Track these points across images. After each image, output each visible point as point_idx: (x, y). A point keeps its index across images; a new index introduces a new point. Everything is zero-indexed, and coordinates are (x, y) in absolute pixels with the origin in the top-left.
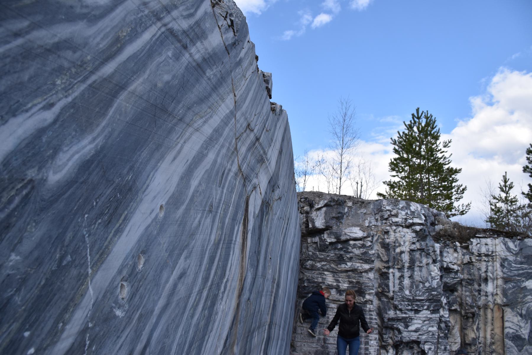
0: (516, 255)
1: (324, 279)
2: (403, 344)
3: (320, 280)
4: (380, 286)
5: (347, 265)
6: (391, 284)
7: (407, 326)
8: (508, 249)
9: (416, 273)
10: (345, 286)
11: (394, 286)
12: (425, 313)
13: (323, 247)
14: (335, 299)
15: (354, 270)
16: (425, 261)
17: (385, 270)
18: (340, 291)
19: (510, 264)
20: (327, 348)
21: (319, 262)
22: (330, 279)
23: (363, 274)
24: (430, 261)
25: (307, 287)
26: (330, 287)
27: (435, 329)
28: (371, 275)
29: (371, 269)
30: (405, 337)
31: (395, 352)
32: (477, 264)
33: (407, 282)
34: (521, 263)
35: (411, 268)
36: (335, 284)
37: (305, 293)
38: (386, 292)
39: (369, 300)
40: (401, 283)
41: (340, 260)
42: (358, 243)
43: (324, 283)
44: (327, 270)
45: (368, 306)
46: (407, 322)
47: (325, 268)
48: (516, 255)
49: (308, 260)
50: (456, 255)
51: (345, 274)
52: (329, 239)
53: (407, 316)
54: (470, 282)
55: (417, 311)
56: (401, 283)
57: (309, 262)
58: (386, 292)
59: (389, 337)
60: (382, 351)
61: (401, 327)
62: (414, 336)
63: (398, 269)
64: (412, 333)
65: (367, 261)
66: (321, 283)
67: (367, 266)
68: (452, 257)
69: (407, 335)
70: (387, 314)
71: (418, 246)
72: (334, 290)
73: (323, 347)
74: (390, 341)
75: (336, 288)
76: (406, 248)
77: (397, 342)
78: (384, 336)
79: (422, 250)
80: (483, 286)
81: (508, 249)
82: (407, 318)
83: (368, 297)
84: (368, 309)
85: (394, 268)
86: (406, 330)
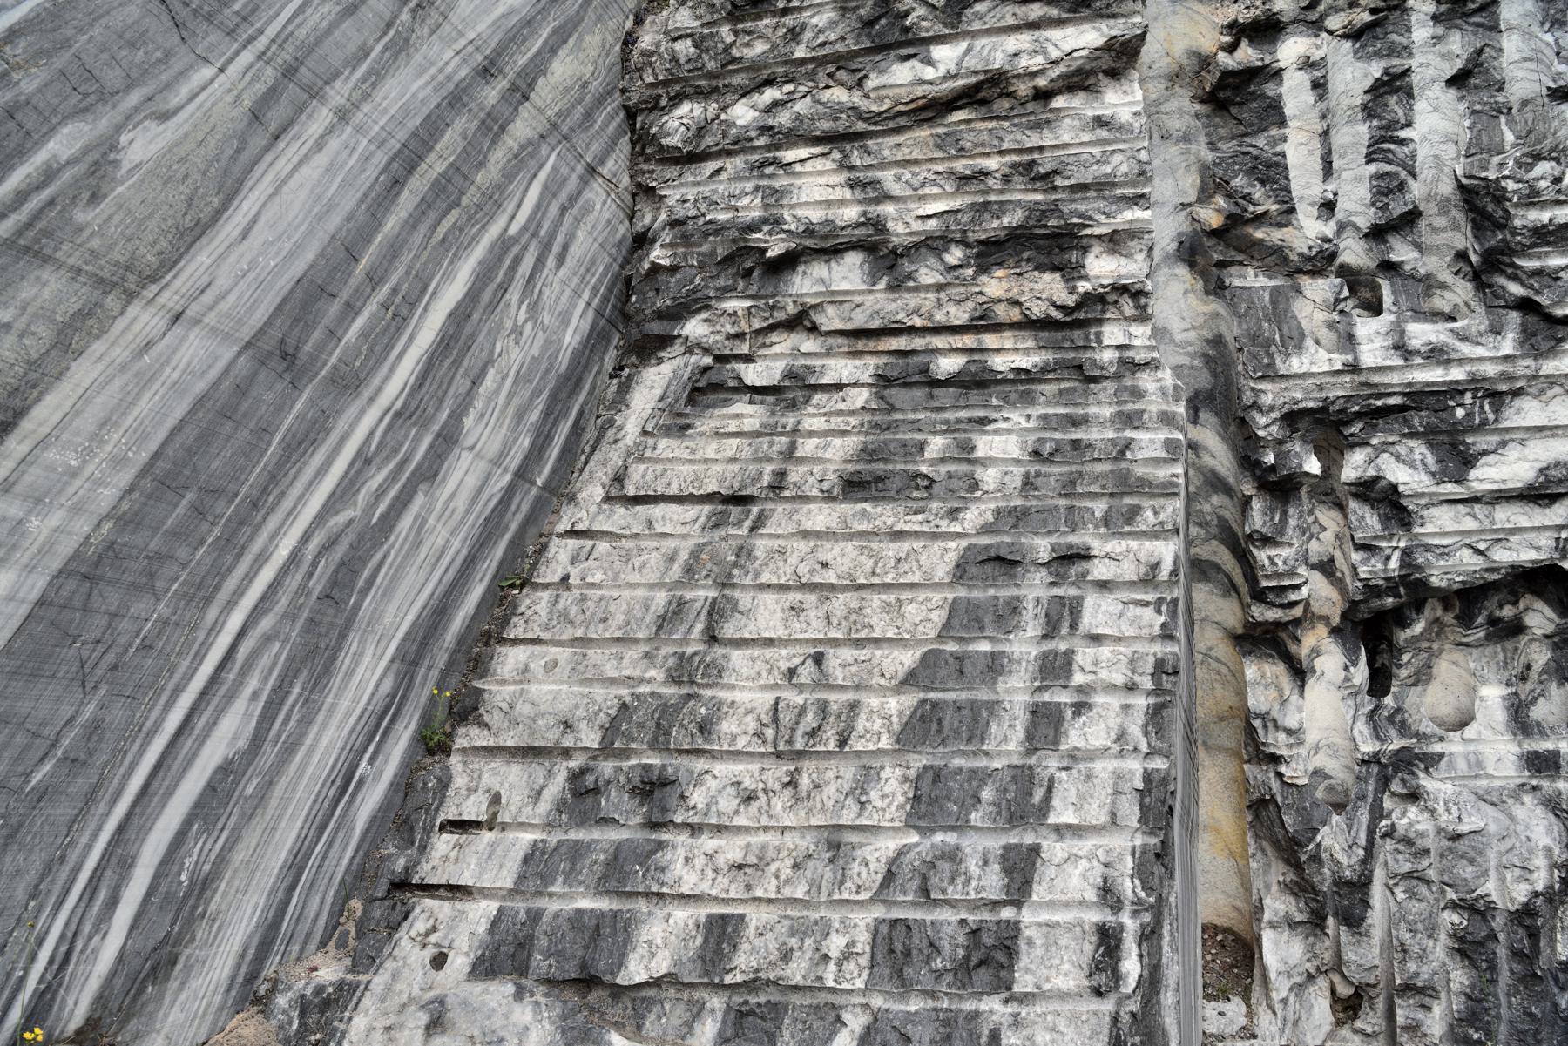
1: (775, 196)
2: (1433, 609)
3: (752, 209)
4: (1212, 184)
5: (929, 62)
6: (1298, 150)
7: (1457, 458)
9: (1511, 45)
11: (1328, 170)
14: (859, 320)
15: (985, 92)
17: (1248, 54)
18: (887, 258)
20: (716, 672)
21: (745, 93)
22: (817, 190)
23: (1059, 102)
25: (673, 269)
26: (824, 245)
28: (1121, 101)
30: (1444, 552)
31: (1361, 674)
36: (851, 213)
37: (660, 315)
38: (1260, 219)
39: (1123, 289)
40: (1386, 142)
43: (777, 221)
44: (794, 137)
45: (1113, 334)
47: (784, 118)
49: (677, 100)
51: (924, 133)
53: (1457, 374)
56: (1386, 142)
57: (684, 108)
58: (1260, 219)
59: (1304, 558)
60: (1251, 671)
61: (1406, 467)
63: (1354, 34)
64: (1507, 515)
66: (753, 227)
70: (1270, 375)
72: (854, 259)
73: (682, 671)
74: (1318, 591)
75: (868, 247)
77: (1372, 591)
78: (1262, 555)
82: (1454, 391)
83: (1101, 268)
84: (1108, 356)
85: (1317, 27)
86: (1450, 488)
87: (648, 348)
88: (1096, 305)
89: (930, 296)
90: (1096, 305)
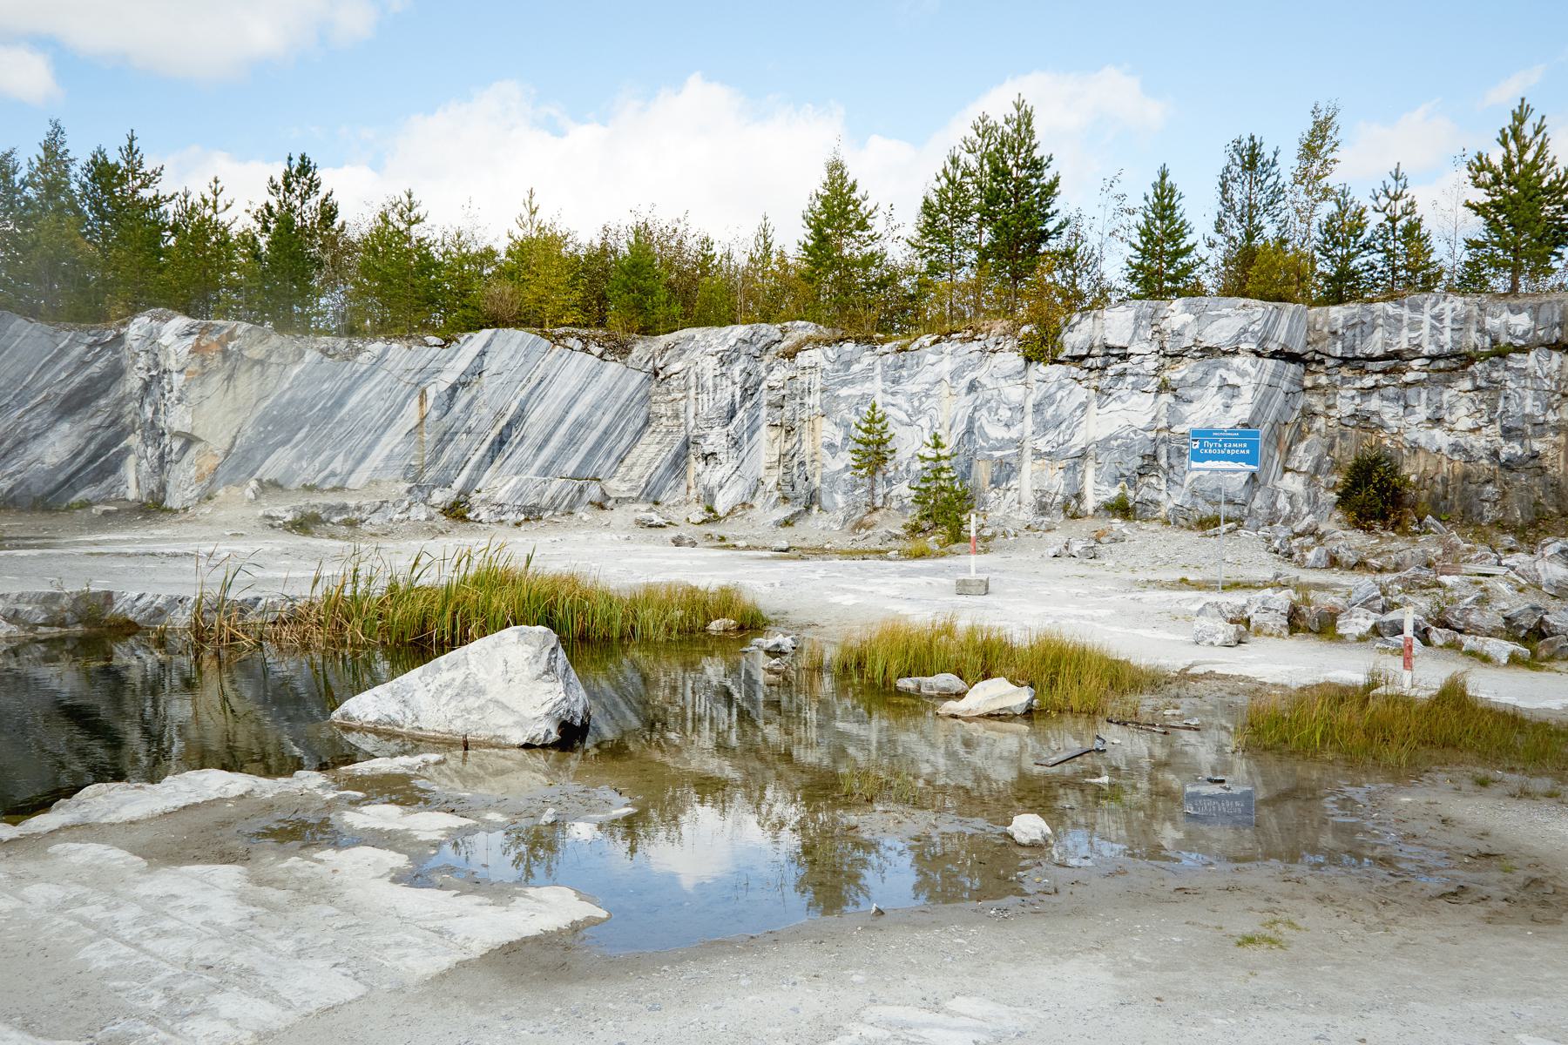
12: (717, 429)
32: (801, 378)
41: (668, 393)
52: (661, 376)
54: (793, 396)
68: (779, 375)
69: (708, 450)
76: (709, 374)
79: (723, 374)
80: (806, 400)
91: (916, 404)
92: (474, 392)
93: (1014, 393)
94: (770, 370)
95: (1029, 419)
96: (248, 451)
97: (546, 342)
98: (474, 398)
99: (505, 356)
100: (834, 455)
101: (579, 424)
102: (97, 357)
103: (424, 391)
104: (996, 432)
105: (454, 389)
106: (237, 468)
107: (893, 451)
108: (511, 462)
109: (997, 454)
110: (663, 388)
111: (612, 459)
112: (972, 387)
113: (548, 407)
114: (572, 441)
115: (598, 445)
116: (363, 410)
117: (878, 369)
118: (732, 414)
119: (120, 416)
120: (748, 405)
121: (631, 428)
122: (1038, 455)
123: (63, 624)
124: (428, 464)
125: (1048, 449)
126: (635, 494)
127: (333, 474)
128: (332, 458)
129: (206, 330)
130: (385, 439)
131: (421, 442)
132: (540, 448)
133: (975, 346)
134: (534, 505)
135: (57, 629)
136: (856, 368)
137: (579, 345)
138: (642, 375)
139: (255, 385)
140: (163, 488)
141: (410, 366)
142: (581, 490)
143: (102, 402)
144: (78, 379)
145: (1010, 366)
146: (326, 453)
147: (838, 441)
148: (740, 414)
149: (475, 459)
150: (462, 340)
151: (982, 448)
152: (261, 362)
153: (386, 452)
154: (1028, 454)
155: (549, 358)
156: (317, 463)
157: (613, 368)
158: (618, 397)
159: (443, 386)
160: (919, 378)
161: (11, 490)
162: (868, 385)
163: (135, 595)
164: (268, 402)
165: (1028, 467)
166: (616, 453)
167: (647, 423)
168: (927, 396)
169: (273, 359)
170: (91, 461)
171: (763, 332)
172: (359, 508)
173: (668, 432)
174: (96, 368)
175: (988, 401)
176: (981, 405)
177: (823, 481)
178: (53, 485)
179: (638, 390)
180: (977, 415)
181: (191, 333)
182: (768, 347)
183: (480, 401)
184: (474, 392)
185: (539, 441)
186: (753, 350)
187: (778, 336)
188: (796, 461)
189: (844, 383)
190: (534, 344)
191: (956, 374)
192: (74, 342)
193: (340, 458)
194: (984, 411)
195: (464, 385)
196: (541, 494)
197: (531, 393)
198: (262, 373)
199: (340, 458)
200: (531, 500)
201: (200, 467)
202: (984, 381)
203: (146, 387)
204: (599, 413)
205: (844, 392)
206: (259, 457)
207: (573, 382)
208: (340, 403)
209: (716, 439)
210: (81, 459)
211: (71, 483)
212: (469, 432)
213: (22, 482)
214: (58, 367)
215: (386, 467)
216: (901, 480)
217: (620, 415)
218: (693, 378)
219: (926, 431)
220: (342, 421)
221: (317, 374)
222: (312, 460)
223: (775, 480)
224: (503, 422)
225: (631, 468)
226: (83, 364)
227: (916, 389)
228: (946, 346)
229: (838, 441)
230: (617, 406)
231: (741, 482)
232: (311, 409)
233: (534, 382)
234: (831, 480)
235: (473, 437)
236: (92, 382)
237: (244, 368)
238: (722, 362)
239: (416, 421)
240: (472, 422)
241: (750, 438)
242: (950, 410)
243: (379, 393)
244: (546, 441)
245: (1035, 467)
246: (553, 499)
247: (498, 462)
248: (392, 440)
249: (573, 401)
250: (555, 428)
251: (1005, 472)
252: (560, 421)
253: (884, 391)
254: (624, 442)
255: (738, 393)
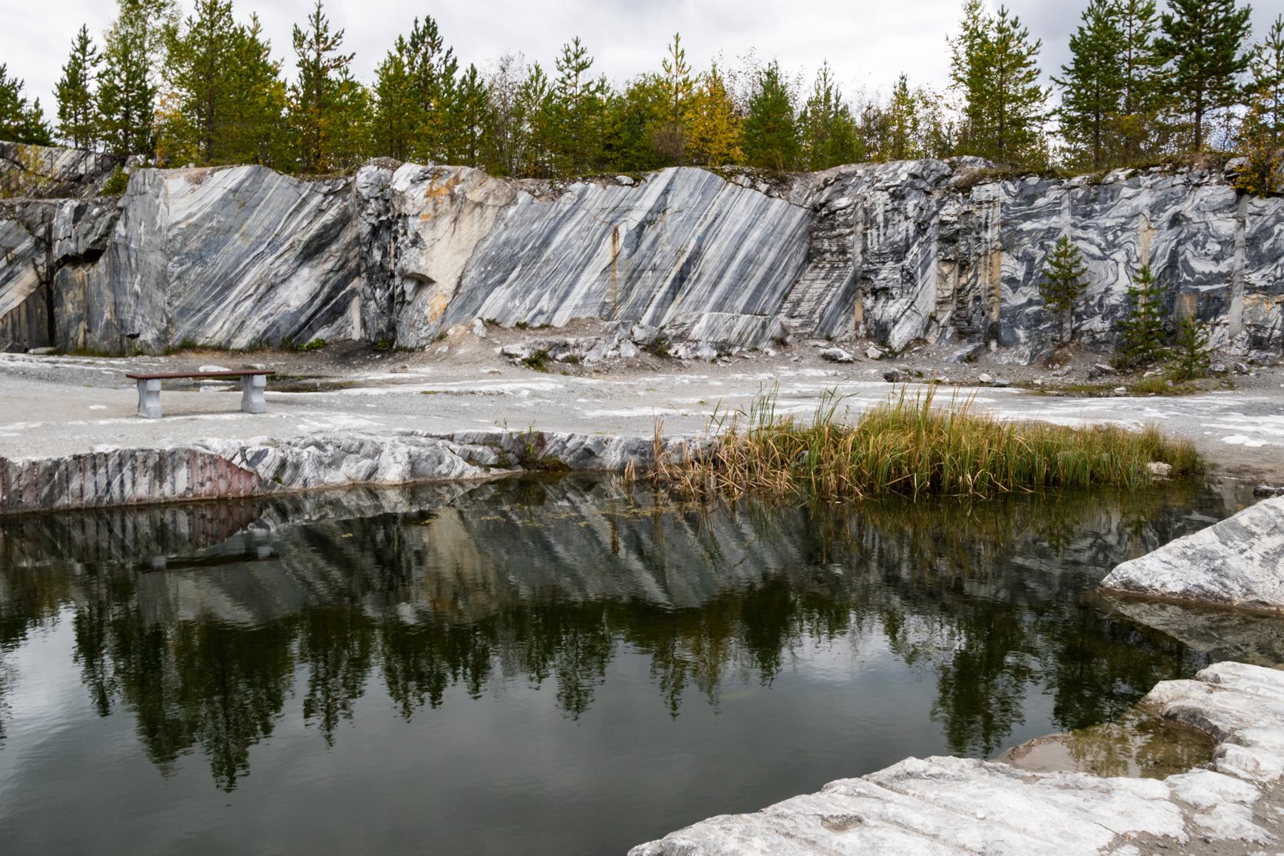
0: (1015, 197)
8: (1008, 192)
10: (834, 249)
12: (890, 264)
13: (821, 220)
15: (841, 235)
16: (897, 218)
18: (832, 254)
19: (1008, 208)
22: (826, 245)
24: (902, 217)
26: (826, 251)
27: (898, 276)
28: (851, 237)
29: (852, 233)
32: (978, 213)
33: (882, 239)
34: (1020, 205)
35: (886, 226)
41: (833, 228)
42: (842, 212)
46: (876, 272)
48: (1015, 197)
50: (957, 206)
52: (824, 212)
54: (967, 231)
55: (884, 263)
62: (883, 284)
65: (849, 226)
67: (848, 231)
68: (950, 211)
69: (879, 284)
71: (889, 208)
76: (880, 210)
79: (895, 209)
80: (983, 234)
81: (1008, 192)
87: (810, 262)
88: (849, 260)
89: (835, 258)
90: (849, 260)
91: (1110, 237)
92: (658, 230)
93: (1225, 226)
94: (941, 204)
95: (1239, 254)
96: (472, 291)
97: (720, 179)
98: (658, 236)
99: (685, 194)
100: (1015, 289)
101: (749, 261)
102: (331, 204)
103: (616, 230)
104: (1203, 266)
105: (642, 226)
106: (462, 307)
107: (1085, 285)
108: (690, 298)
109: (1204, 288)
110: (827, 224)
111: (777, 295)
112: (1176, 220)
113: (721, 244)
114: (742, 277)
115: (765, 280)
116: (565, 249)
117: (1067, 203)
118: (908, 247)
119: (347, 261)
120: (921, 239)
121: (793, 264)
122: (1252, 289)
123: (507, 465)
124: (620, 302)
125: (1263, 283)
126: (809, 330)
127: (541, 312)
128: (540, 297)
129: (437, 175)
130: (583, 277)
131: (614, 280)
132: (715, 284)
133: (1179, 180)
134: (725, 342)
135: (504, 471)
136: (1040, 202)
137: (747, 182)
138: (803, 210)
139: (476, 226)
140: (392, 327)
141: (605, 205)
142: (764, 326)
143: (334, 247)
144: (317, 226)
145: (1220, 199)
146: (535, 292)
147: (1020, 275)
148: (915, 249)
149: (659, 296)
150: (649, 179)
151: (1186, 282)
152: (480, 205)
153: (585, 290)
154: (1238, 288)
155: (723, 195)
156: (527, 302)
157: (778, 204)
158: (782, 233)
159: (633, 224)
160: (1113, 212)
161: (265, 332)
162: (1054, 218)
163: (565, 435)
164: (486, 244)
165: (1239, 304)
166: (780, 290)
167: (809, 258)
168: (1123, 230)
169: (490, 201)
170: (325, 303)
171: (933, 166)
172: (577, 346)
173: (833, 268)
174: (328, 217)
175: (1195, 235)
176: (1186, 239)
177: (1002, 314)
178: (296, 327)
179: (799, 226)
180: (1181, 249)
181: (425, 179)
182: (937, 182)
183: (664, 239)
184: (658, 230)
185: (714, 278)
186: (923, 185)
187: (947, 171)
188: (971, 295)
189: (1027, 217)
190: (710, 181)
191: (1156, 208)
192: (314, 192)
193: (547, 296)
194: (1189, 246)
195: (651, 222)
196: (730, 330)
197: (707, 230)
198: (482, 215)
199: (547, 296)
200: (722, 336)
201: (433, 307)
202: (1189, 215)
203: (375, 231)
204: (766, 249)
205: (1027, 226)
206: (480, 297)
207: (743, 219)
208: (546, 243)
209: (888, 274)
210: (318, 302)
211: (310, 325)
212: (654, 269)
213: (273, 324)
214: (301, 216)
215: (585, 305)
216: (1093, 314)
217: (784, 251)
218: (861, 213)
219: (1122, 266)
220: (548, 260)
221: (528, 215)
222: (524, 298)
223: (948, 315)
224: (683, 260)
225: (797, 303)
226: (320, 211)
227: (1109, 223)
228: (1145, 180)
229: (1020, 275)
230: (782, 242)
231: (915, 317)
232: (523, 248)
233: (710, 219)
234: (1013, 316)
235: (657, 274)
236: (326, 228)
237: (467, 210)
238: (894, 196)
239: (609, 259)
240: (657, 260)
241: (923, 273)
242: (1151, 242)
243: (579, 232)
244: (720, 277)
245: (1248, 302)
246: (741, 335)
247: (679, 298)
248: (589, 279)
249: (743, 236)
250: (728, 265)
251: (1213, 306)
252: (732, 258)
253: (1074, 225)
254: (787, 278)
255: (912, 228)
